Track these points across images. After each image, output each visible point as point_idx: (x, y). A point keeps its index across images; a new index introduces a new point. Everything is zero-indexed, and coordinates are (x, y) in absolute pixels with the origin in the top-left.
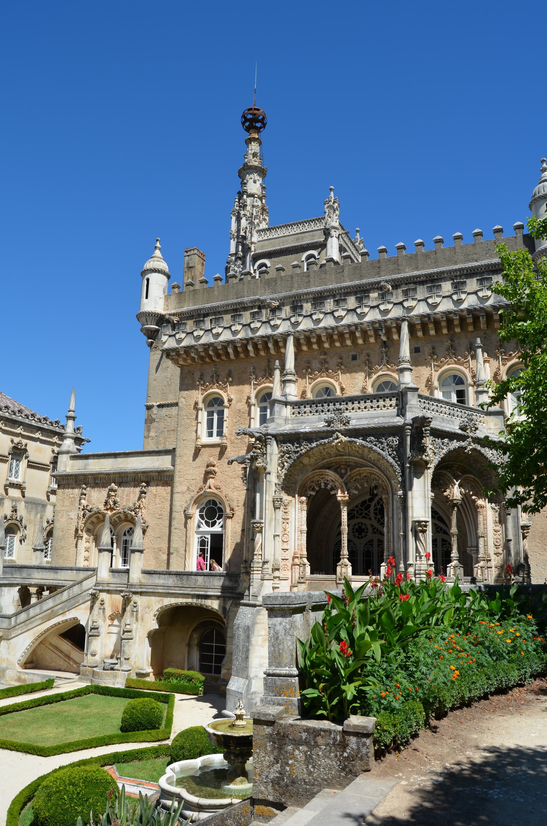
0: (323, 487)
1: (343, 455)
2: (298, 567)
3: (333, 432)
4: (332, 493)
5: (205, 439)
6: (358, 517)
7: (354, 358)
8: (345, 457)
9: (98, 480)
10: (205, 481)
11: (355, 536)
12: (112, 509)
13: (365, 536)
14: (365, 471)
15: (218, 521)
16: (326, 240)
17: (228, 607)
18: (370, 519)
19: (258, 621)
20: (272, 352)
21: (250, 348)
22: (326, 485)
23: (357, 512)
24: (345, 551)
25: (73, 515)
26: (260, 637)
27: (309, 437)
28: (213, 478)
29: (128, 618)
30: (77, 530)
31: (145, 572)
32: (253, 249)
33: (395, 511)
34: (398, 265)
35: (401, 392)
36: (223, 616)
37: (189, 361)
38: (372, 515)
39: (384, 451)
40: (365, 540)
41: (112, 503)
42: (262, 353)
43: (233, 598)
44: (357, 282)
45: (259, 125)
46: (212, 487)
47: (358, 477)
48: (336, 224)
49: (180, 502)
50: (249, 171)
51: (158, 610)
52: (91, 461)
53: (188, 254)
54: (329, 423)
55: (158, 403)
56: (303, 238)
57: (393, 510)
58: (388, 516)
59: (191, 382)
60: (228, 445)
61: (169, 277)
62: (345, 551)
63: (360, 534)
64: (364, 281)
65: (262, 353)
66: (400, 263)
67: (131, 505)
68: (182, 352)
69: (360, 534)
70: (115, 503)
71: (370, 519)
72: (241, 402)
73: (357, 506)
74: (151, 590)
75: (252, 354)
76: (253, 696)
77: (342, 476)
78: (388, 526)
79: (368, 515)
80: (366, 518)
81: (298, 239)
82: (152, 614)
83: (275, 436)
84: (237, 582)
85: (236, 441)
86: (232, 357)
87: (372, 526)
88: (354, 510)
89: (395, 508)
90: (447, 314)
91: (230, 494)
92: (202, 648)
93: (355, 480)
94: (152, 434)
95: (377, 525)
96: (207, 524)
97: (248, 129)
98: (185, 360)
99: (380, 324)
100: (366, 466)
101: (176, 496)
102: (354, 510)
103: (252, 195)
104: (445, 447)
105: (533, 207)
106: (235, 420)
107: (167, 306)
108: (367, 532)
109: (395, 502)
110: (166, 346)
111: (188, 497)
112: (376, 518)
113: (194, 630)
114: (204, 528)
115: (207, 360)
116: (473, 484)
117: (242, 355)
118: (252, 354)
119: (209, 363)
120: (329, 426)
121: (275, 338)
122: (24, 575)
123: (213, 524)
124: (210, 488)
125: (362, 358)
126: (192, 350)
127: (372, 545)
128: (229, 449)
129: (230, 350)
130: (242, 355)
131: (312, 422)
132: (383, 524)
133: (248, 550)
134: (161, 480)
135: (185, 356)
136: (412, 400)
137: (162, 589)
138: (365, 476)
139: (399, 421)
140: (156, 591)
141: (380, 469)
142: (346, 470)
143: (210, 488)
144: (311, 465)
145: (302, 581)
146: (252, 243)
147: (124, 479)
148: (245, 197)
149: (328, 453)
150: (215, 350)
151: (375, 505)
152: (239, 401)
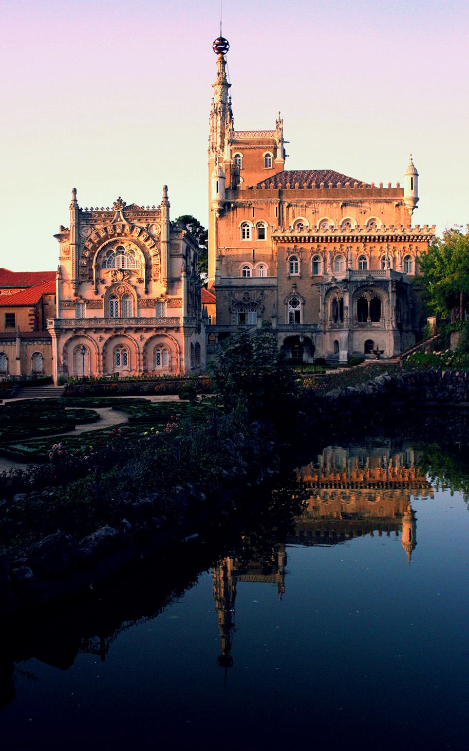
3: (368, 281)
5: (292, 275)
17: (313, 336)
24: (369, 315)
25: (226, 303)
30: (230, 309)
41: (247, 299)
49: (281, 299)
52: (232, 280)
55: (226, 248)
62: (369, 315)
67: (256, 299)
70: (249, 298)
82: (282, 340)
84: (316, 327)
92: (293, 352)
94: (223, 263)
98: (281, 241)
101: (280, 296)
107: (227, 197)
111: (284, 297)
114: (292, 308)
122: (211, 329)
123: (296, 307)
152: (305, 259)
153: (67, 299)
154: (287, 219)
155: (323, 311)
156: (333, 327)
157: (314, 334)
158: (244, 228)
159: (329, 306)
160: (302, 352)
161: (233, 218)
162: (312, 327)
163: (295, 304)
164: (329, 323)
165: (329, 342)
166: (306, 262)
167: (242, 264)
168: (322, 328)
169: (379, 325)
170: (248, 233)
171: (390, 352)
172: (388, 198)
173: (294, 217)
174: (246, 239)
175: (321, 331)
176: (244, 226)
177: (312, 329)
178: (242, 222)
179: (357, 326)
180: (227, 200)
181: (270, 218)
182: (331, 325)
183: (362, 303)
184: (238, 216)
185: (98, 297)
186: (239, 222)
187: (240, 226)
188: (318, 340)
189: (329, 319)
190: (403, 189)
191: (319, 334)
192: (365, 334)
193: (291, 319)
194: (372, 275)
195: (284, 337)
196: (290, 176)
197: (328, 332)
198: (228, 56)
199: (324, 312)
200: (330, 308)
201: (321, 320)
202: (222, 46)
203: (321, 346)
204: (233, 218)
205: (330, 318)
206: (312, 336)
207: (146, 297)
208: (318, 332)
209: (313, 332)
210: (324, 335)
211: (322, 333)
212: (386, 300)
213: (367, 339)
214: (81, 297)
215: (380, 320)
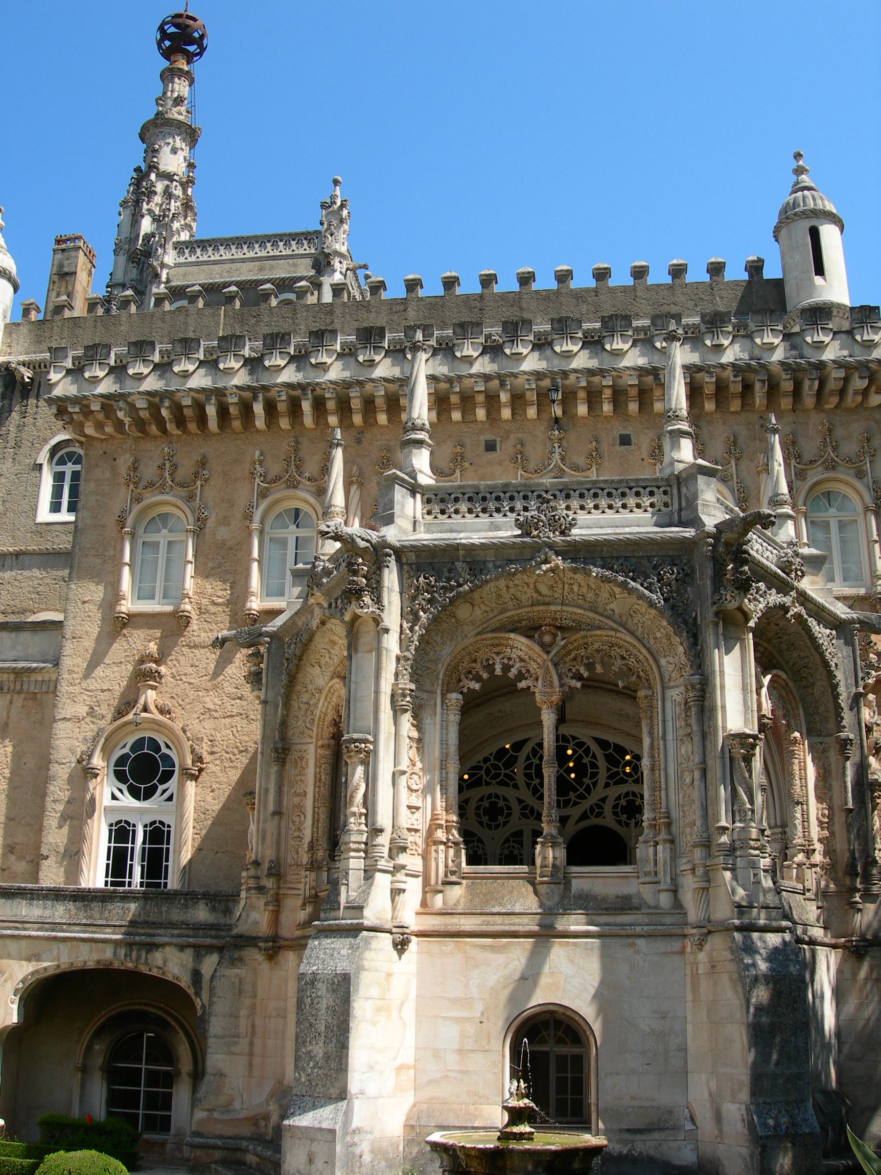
0: (498, 671)
1: (548, 604)
2: (442, 847)
3: (536, 548)
4: (522, 684)
6: (488, 784)
7: (490, 447)
8: (553, 608)
11: (481, 823)
13: (505, 823)
14: (599, 639)
15: (161, 788)
18: (516, 786)
19: (366, 964)
20: (308, 420)
21: (258, 408)
22: (506, 668)
23: (488, 772)
26: (370, 1002)
28: (154, 688)
32: (164, 278)
33: (669, 725)
34: (521, 309)
35: (678, 477)
36: (191, 991)
37: (109, 429)
38: (521, 780)
40: (504, 833)
42: (284, 423)
43: (220, 949)
45: (192, 48)
46: (152, 707)
47: (583, 652)
48: (344, 249)
50: (166, 130)
51: (23, 981)
53: (63, 246)
54: (526, 527)
56: (272, 267)
57: (664, 721)
58: (651, 734)
59: (108, 475)
60: (194, 616)
61: (16, 288)
63: (493, 818)
65: (284, 423)
66: (524, 305)
68: (95, 407)
69: (493, 818)
71: (516, 786)
72: (229, 524)
73: (486, 760)
74: (9, 932)
75: (260, 423)
76: (356, 1139)
77: (546, 648)
78: (652, 757)
79: (513, 779)
80: (508, 785)
81: (261, 269)
82: (10, 987)
83: (399, 552)
84: (228, 912)
85: (213, 609)
86: (213, 424)
87: (520, 801)
88: (481, 768)
89: (669, 718)
91: (195, 727)
92: (112, 1075)
93: (574, 659)
95: (530, 800)
96: (135, 793)
97: (167, 54)
98: (99, 426)
99: (553, 380)
100: (600, 628)
102: (481, 768)
103: (169, 177)
104: (761, 599)
105: (784, 232)
106: (210, 564)
108: (509, 815)
109: (668, 705)
110: (58, 392)
111: (89, 729)
112: (528, 785)
113: (98, 1034)
114: (127, 801)
115: (153, 429)
116: (783, 693)
117: (237, 424)
118: (260, 423)
119: (155, 437)
120: (528, 534)
121: (319, 391)
123: (149, 794)
124: (145, 709)
125: (506, 449)
126: (121, 404)
127: (521, 843)
128: (194, 625)
129: (211, 410)
130: (237, 424)
132: (541, 797)
133: (264, 838)
134: (20, 692)
135: (101, 416)
137: (39, 930)
138: (598, 651)
139: (675, 531)
140: (23, 933)
141: (632, 633)
142: (555, 636)
143: (145, 709)
144: (473, 623)
145: (454, 878)
146: (163, 265)
148: (153, 177)
149: (514, 598)
150: (177, 409)
151: (528, 758)
152: (225, 521)
155: (271, 807)
158: (61, 468)
159: (311, 771)
161: (20, 428)
162: (202, 914)
163: (145, 769)
166: (223, 533)
169: (631, 888)
171: (718, 1118)
175: (250, 941)
176: (62, 462)
177: (199, 928)
178: (53, 442)
179: (456, 893)
184: (40, 422)
186: (46, 441)
187: (43, 457)
189: (305, 859)
190: (778, 285)
191: (234, 962)
193: (118, 864)
199: (278, 813)
200: (317, 780)
201: (257, 863)
202: (180, 40)
203: (244, 1042)
204: (20, 428)
205: (312, 847)
206: (196, 975)
208: (232, 945)
209: (200, 951)
210: (265, 966)
211: (255, 956)
212: (676, 694)
215: (643, 851)
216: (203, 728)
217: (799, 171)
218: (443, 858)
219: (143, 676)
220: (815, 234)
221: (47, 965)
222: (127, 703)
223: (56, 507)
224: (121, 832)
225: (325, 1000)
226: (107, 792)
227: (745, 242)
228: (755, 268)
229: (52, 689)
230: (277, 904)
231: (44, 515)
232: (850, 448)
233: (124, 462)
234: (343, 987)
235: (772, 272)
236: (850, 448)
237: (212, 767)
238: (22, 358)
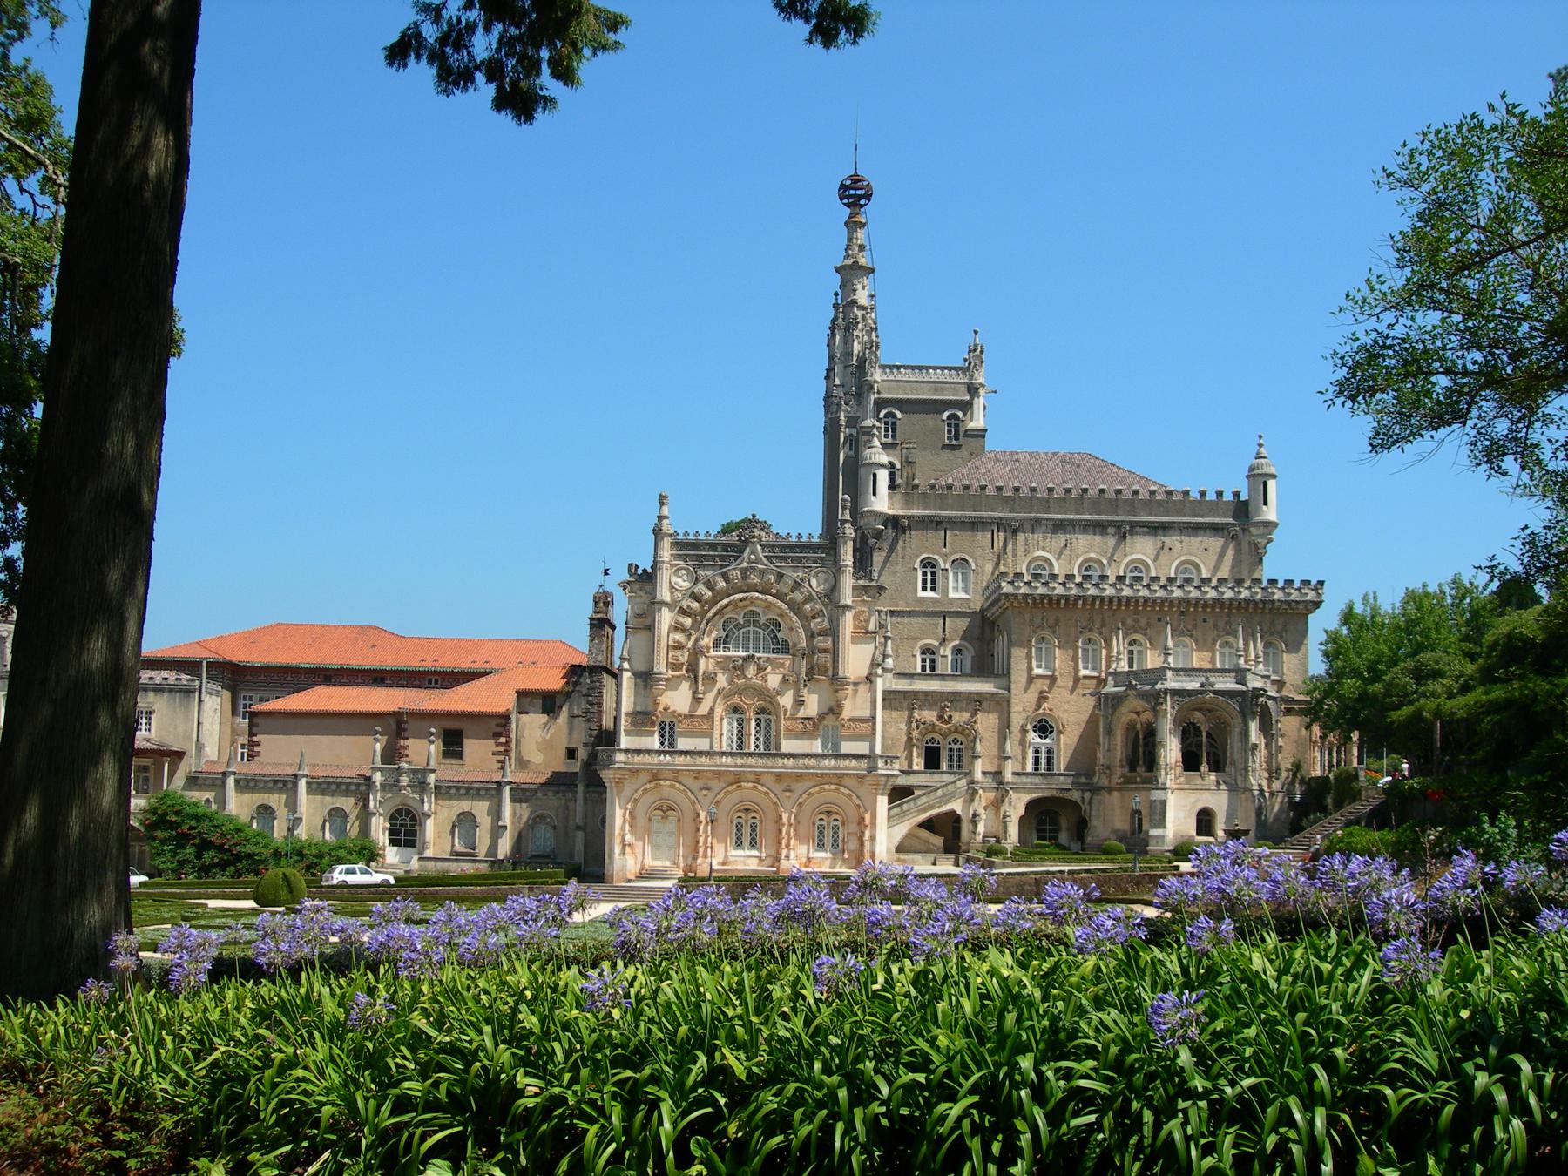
9: (929, 699)
10: (1039, 706)
12: (946, 723)
16: (972, 398)
27: (1189, 693)
29: (1005, 806)
31: (1015, 774)
39: (1234, 705)
44: (1096, 517)
49: (1017, 719)
64: (1103, 517)
90: (1231, 600)
111: (1024, 715)
131: (1193, 684)
136: (1249, 676)
139: (1240, 687)
147: (955, 698)
153: (639, 709)
154: (1014, 555)
156: (1128, 781)
157: (1087, 795)
160: (1057, 831)
161: (904, 548)
163: (1044, 728)
164: (1119, 772)
165: (1117, 812)
167: (920, 643)
168: (1104, 782)
170: (933, 582)
172: (1217, 520)
173: (1027, 551)
174: (929, 594)
180: (891, 512)
181: (979, 552)
182: (1123, 776)
183: (1188, 734)
185: (703, 709)
187: (917, 565)
188: (1094, 807)
192: (1197, 795)
193: (1037, 761)
194: (1212, 680)
195: (1026, 797)
196: (1006, 463)
197: (1119, 789)
198: (870, 212)
202: (855, 194)
204: (904, 548)
207: (801, 714)
208: (1096, 790)
213: (1200, 806)
214: (666, 709)
216: (1065, 716)
217: (1261, 446)
218: (1179, 770)
219: (1042, 698)
220: (1265, 484)
221: (1035, 795)
222: (1039, 706)
223: (924, 589)
224: (1037, 751)
225: (1159, 806)
226: (1033, 737)
227: (1235, 484)
228: (1236, 494)
229: (1009, 702)
230: (1109, 777)
231: (921, 594)
232: (1279, 627)
233: (1028, 617)
234: (1164, 803)
235: (1244, 497)
236: (1279, 627)
237: (1068, 729)
238: (901, 513)
